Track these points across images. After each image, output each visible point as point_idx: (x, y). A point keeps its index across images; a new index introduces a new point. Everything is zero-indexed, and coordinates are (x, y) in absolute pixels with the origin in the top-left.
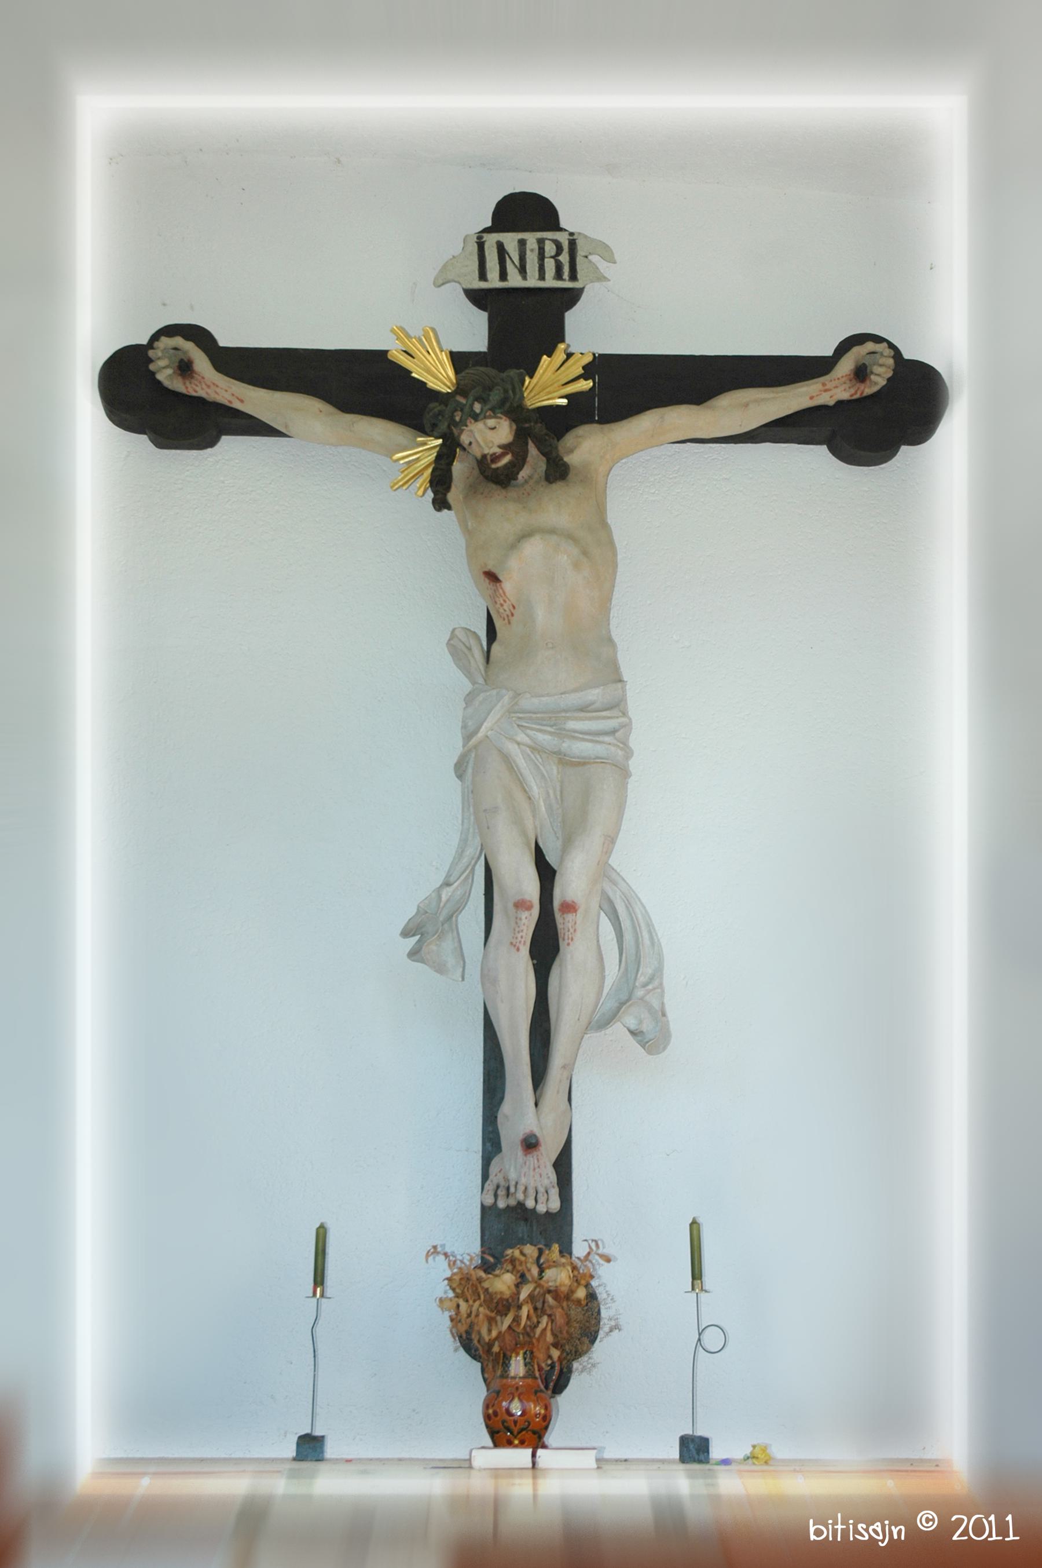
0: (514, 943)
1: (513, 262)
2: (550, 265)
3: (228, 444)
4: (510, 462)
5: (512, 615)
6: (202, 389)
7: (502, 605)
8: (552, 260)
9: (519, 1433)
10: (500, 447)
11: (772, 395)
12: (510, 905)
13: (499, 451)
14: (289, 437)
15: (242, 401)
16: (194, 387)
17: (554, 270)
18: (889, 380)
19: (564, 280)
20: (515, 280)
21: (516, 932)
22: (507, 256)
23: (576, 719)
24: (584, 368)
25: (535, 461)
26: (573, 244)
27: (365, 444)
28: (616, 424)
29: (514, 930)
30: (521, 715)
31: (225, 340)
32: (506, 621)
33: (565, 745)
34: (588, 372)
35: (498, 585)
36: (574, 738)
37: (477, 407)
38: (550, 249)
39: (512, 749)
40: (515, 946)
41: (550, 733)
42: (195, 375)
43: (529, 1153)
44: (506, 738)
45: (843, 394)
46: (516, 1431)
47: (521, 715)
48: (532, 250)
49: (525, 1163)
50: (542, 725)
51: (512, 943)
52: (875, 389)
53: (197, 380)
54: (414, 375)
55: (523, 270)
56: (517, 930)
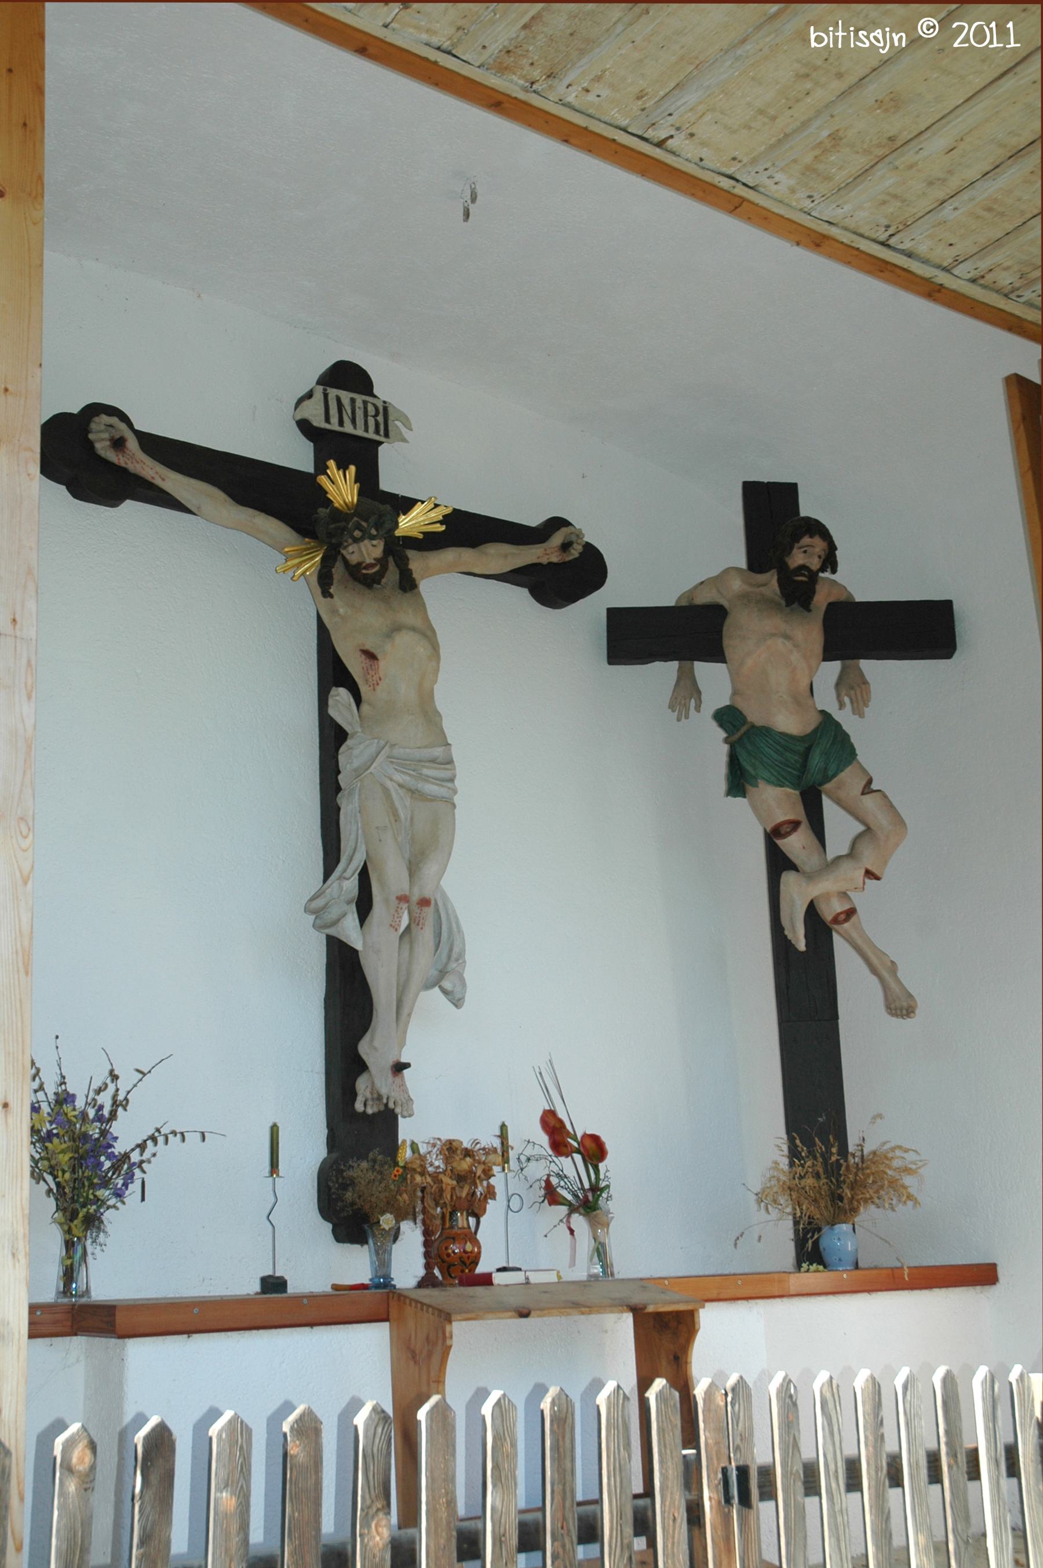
0: (393, 925)
1: (347, 413)
2: (371, 422)
3: (129, 506)
4: (377, 572)
5: (378, 684)
6: (132, 463)
7: (372, 676)
8: (372, 419)
9: (470, 1265)
10: (375, 559)
11: (515, 551)
12: (393, 898)
13: (373, 561)
14: (194, 514)
15: (163, 480)
16: (126, 460)
17: (374, 426)
18: (580, 553)
19: (380, 435)
20: (348, 428)
21: (396, 917)
22: (344, 411)
23: (427, 767)
24: (443, 516)
25: (392, 575)
26: (385, 409)
27: (255, 533)
28: (431, 552)
29: (394, 915)
30: (394, 760)
31: (137, 427)
32: (372, 687)
33: (421, 785)
34: (446, 520)
35: (376, 662)
36: (426, 781)
37: (374, 532)
38: (371, 410)
39: (389, 784)
40: (394, 927)
41: (410, 775)
42: (126, 450)
43: (397, 1075)
44: (385, 775)
45: (555, 559)
46: (468, 1263)
47: (394, 760)
48: (359, 408)
49: (394, 1082)
50: (406, 769)
51: (391, 925)
52: (571, 558)
53: (129, 455)
54: (329, 496)
55: (354, 421)
56: (396, 915)
